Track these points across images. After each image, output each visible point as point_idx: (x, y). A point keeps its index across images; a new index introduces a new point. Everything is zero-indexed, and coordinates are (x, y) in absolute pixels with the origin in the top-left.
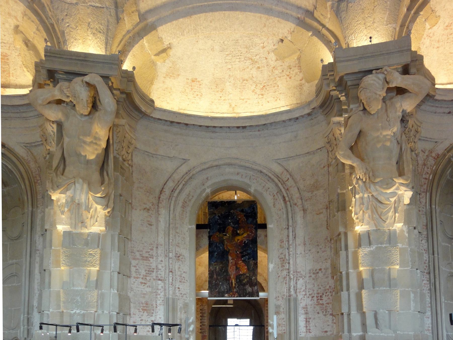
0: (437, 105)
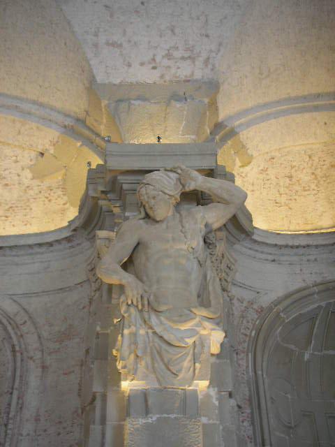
0: (256, 248)
